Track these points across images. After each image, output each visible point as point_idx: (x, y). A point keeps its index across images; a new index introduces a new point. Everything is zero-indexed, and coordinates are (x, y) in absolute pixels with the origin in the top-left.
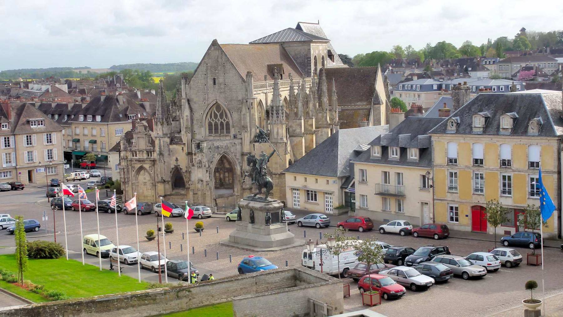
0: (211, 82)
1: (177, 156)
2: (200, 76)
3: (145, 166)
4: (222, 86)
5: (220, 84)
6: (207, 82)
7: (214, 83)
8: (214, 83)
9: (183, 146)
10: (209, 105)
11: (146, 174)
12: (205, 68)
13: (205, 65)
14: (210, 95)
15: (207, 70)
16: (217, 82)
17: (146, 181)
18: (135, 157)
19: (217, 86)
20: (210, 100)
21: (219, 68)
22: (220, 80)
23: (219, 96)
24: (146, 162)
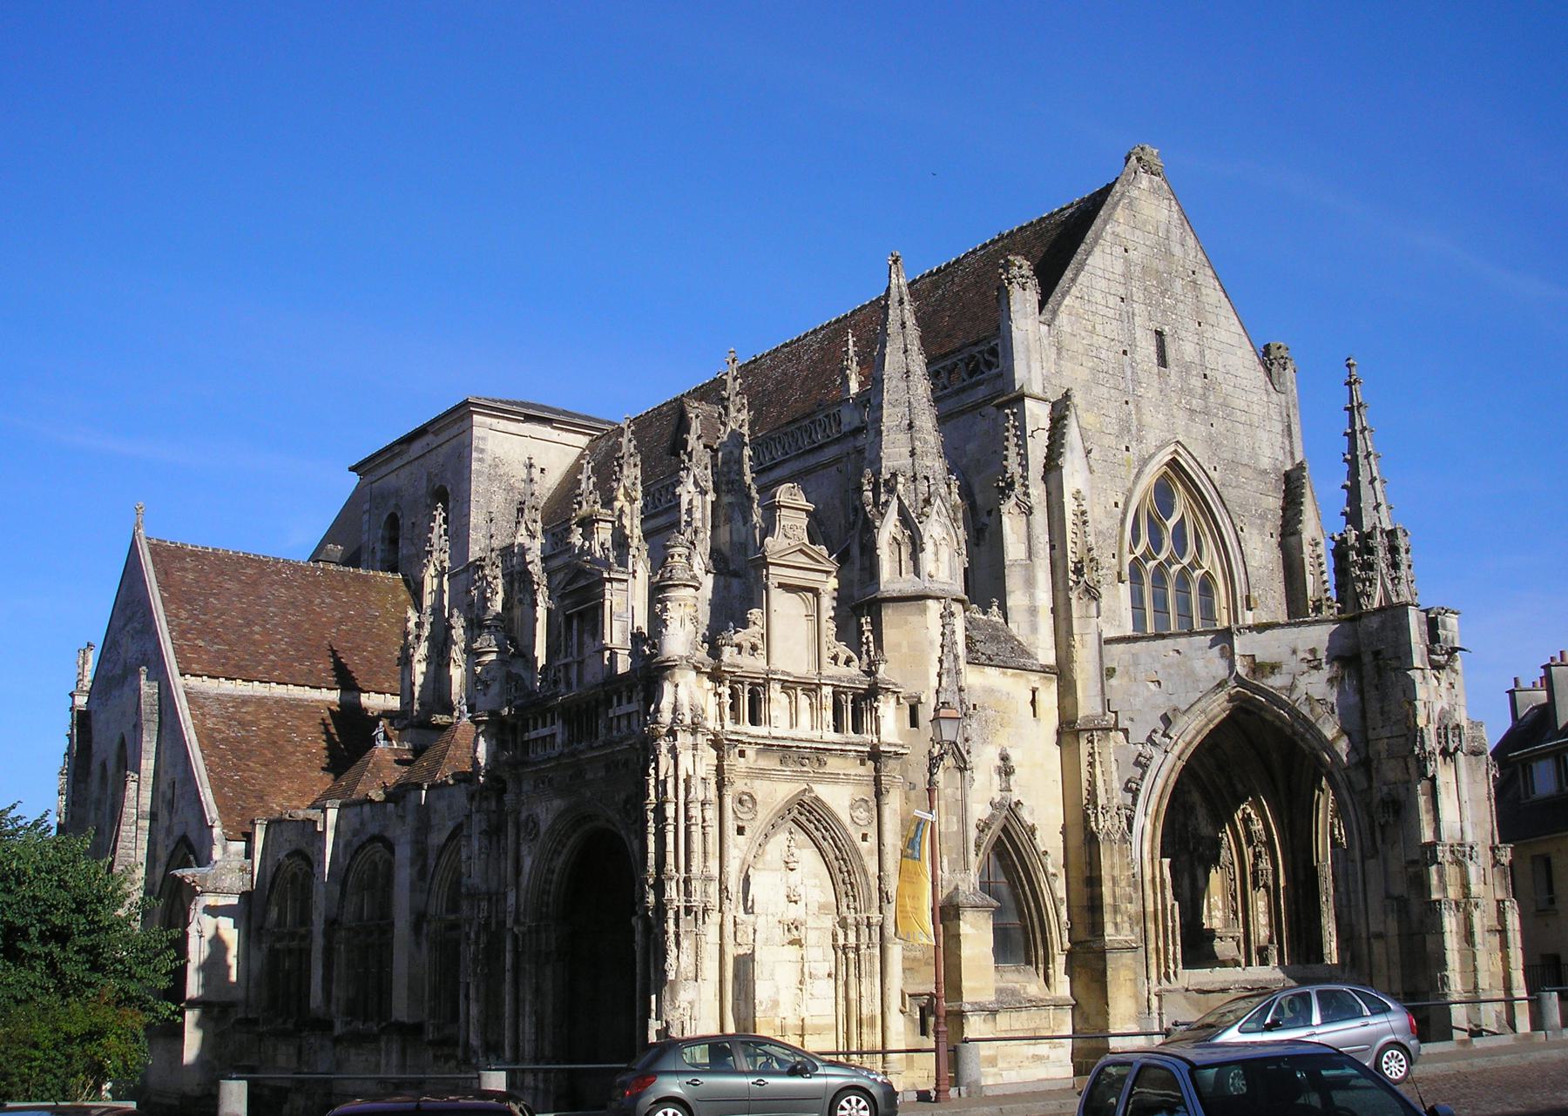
0: (1146, 348)
1: (1004, 739)
2: (1098, 297)
3: (823, 791)
4: (1196, 383)
5: (1186, 368)
6: (1133, 343)
7: (1163, 361)
8: (1163, 361)
9: (1035, 680)
10: (1144, 462)
11: (808, 858)
12: (1119, 267)
13: (1119, 250)
14: (1147, 419)
15: (1127, 277)
16: (1171, 353)
17: (794, 912)
18: (761, 730)
19: (1173, 371)
20: (1152, 440)
21: (1178, 283)
22: (1183, 348)
23: (1187, 431)
24: (833, 764)
